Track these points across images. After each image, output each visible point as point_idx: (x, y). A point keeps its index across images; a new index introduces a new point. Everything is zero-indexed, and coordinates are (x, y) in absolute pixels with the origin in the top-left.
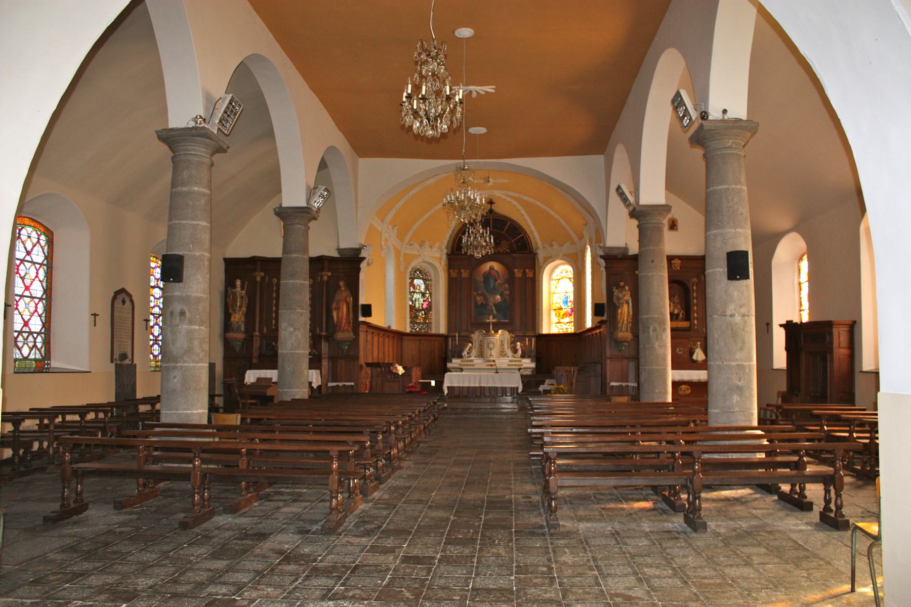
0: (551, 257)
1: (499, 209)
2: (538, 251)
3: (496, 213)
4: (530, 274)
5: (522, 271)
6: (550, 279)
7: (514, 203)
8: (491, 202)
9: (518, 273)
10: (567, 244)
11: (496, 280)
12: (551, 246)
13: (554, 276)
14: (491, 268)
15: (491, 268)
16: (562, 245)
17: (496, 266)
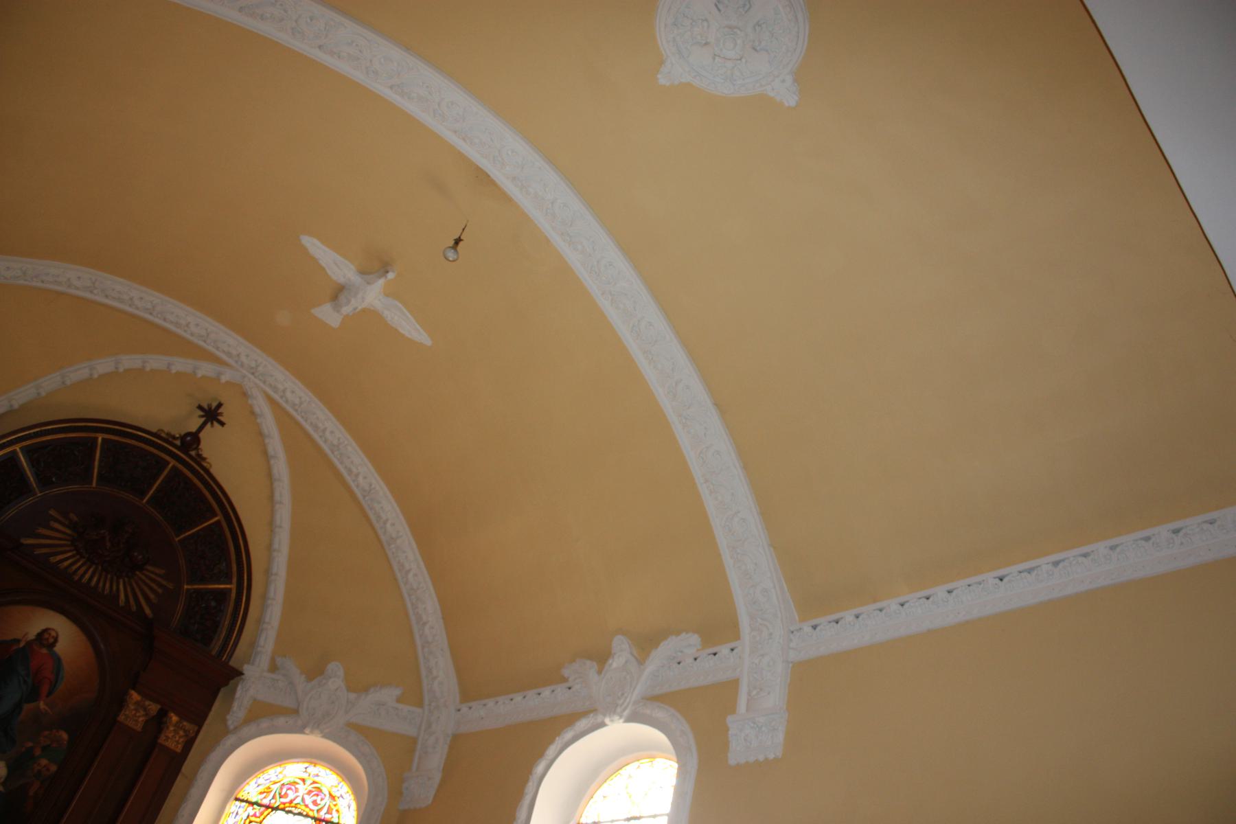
0: (296, 712)
1: (223, 454)
2: (247, 670)
3: (200, 459)
4: (172, 739)
5: (154, 708)
6: (231, 794)
7: (281, 467)
8: (212, 415)
9: (136, 711)
10: (388, 695)
11: (33, 695)
12: (315, 672)
13: (251, 790)
14: (46, 639)
15: (46, 639)
16: (358, 687)
17: (67, 637)
